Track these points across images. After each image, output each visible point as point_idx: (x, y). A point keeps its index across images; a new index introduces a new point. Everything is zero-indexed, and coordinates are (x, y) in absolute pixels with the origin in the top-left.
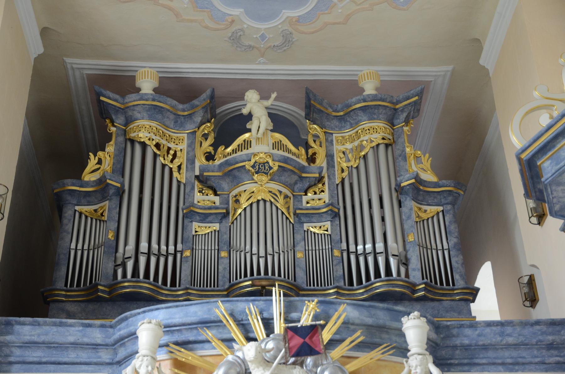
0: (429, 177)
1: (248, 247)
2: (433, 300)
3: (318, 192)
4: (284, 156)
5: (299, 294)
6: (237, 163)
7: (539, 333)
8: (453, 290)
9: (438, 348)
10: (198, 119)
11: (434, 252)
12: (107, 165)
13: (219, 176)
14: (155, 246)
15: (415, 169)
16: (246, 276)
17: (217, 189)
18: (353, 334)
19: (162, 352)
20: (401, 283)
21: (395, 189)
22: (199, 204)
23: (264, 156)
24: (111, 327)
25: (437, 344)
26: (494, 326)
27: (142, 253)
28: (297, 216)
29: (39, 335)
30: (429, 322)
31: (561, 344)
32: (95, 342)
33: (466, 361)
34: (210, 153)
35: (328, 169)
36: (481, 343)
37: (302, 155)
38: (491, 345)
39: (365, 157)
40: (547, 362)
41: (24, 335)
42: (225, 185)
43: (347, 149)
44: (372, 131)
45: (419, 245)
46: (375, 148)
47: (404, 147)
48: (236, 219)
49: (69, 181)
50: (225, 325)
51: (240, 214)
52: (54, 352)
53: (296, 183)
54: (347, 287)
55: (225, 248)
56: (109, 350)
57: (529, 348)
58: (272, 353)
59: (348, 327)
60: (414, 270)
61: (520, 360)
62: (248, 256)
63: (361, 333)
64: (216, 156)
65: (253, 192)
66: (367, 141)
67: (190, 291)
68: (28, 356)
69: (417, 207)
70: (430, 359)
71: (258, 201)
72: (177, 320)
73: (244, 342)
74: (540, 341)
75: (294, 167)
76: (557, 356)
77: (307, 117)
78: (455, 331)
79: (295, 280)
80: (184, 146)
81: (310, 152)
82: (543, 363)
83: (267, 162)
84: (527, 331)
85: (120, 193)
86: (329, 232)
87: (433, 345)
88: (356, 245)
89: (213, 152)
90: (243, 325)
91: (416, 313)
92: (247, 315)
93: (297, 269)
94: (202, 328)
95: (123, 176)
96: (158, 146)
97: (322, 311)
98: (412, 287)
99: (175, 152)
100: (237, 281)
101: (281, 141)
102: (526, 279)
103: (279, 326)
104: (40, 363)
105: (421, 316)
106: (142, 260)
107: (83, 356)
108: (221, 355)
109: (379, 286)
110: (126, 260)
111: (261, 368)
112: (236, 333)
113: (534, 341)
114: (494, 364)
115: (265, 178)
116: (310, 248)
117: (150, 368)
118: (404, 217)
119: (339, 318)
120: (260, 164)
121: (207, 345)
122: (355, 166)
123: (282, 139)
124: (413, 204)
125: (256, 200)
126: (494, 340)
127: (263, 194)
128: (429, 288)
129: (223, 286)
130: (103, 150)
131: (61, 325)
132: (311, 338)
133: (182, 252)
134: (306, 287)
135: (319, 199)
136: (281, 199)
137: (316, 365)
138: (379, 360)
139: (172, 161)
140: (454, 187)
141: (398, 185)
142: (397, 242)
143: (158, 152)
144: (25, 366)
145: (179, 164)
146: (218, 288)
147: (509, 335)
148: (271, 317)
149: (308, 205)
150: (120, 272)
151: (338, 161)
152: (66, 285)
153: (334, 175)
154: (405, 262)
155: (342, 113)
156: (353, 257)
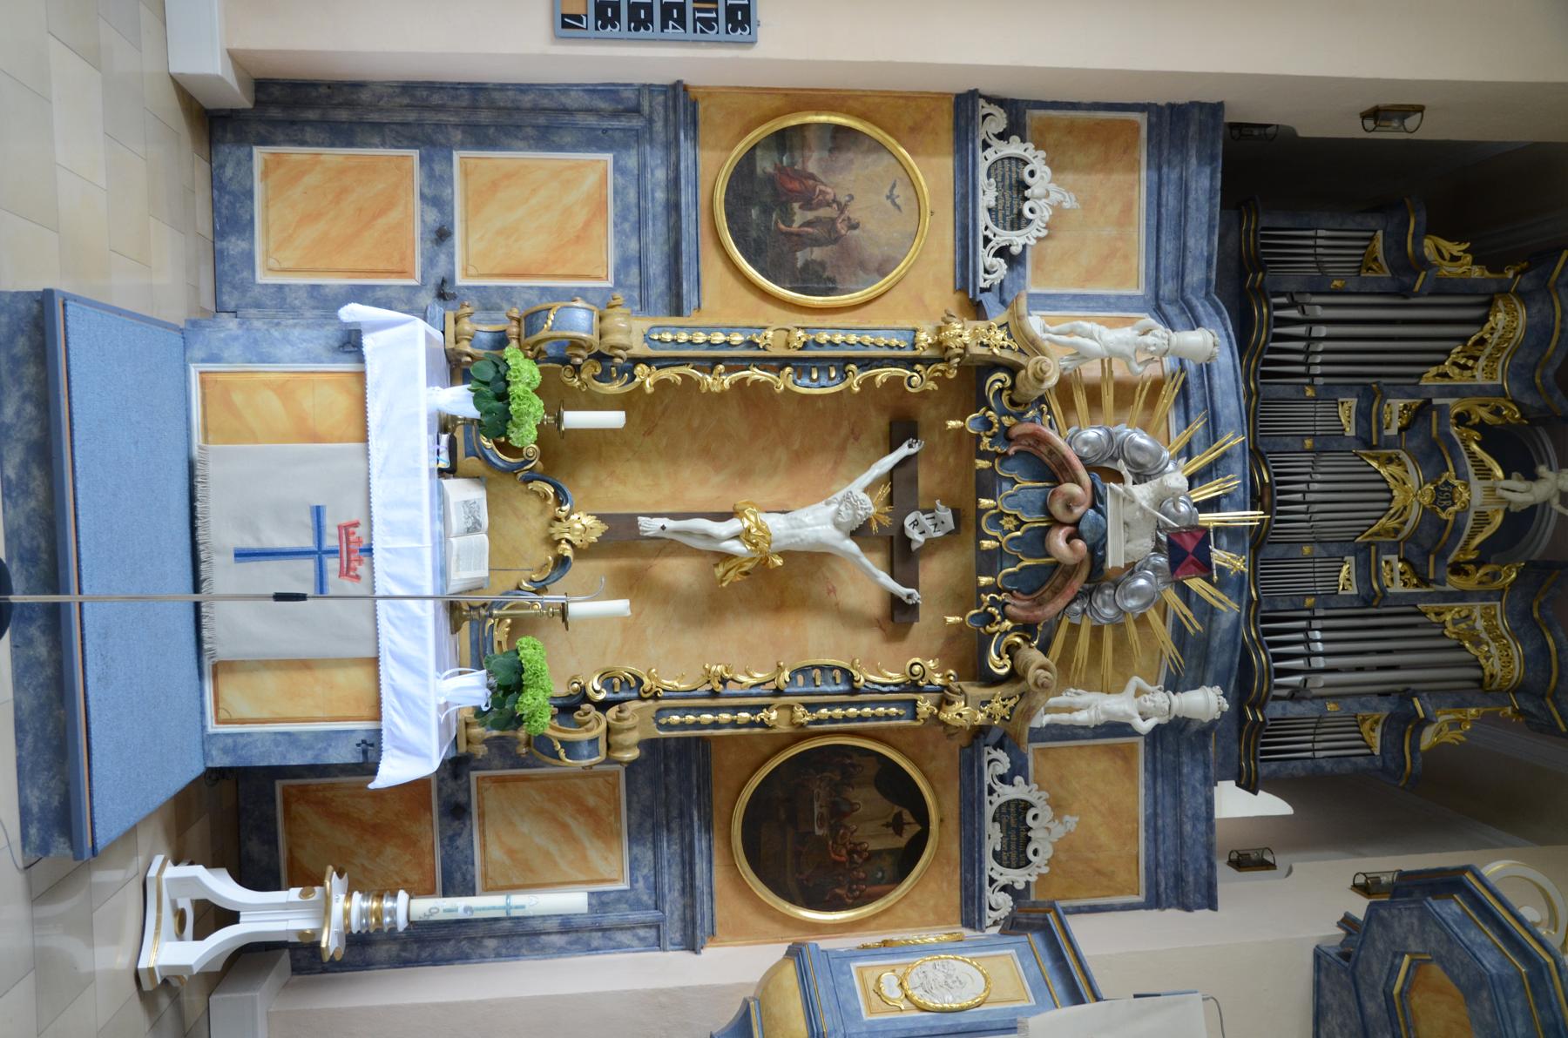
0: (1428, 738)
1: (1319, 477)
2: (1240, 731)
3: (1403, 578)
4: (1464, 529)
6: (1453, 460)
7: (1198, 866)
8: (1255, 759)
10: (1527, 400)
11: (1311, 737)
12: (1448, 270)
13: (1431, 434)
14: (1321, 346)
15: (1442, 719)
16: (1277, 474)
17: (1409, 431)
20: (1265, 689)
21: (1408, 689)
22: (1386, 406)
23: (1463, 499)
24: (1207, 294)
25: (1182, 731)
26: (1207, 809)
27: (1311, 329)
28: (1365, 547)
29: (1196, 200)
30: (1214, 722)
31: (1182, 892)
33: (1159, 767)
34: (1469, 418)
35: (1442, 592)
36: (1184, 789)
37: (1464, 554)
38: (1181, 801)
39: (1461, 648)
40: (1159, 870)
41: (1197, 181)
42: (1414, 443)
43: (1475, 621)
44: (1505, 659)
45: (1320, 717)
46: (1477, 663)
47: (1476, 706)
48: (1362, 460)
49: (1423, 217)
50: (1210, 446)
51: (1370, 465)
52: (1173, 223)
53: (1419, 545)
54: (1260, 615)
55: (1318, 445)
56: (1175, 294)
57: (1176, 850)
58: (1173, 510)
60: (1284, 708)
61: (1161, 837)
62: (1307, 478)
64: (1463, 428)
65: (1405, 484)
66: (1489, 651)
67: (1254, 399)
68: (1168, 190)
69: (1378, 720)
70: (1164, 720)
71: (1390, 491)
72: (1218, 382)
73: (1186, 473)
74: (1186, 866)
75: (1445, 544)
76: (1166, 884)
77: (1531, 564)
78: (1199, 756)
79: (1269, 543)
80: (1481, 379)
81: (1471, 568)
82: (1157, 866)
83: (1454, 504)
84: (1200, 851)
85: (1405, 291)
86: (1341, 592)
88: (1322, 630)
89: (1470, 423)
90: (1211, 471)
91: (1226, 706)
92: (1224, 476)
93: (1286, 546)
94: (1206, 415)
95: (1431, 294)
96: (1482, 342)
97: (1230, 580)
98: (1259, 704)
99: (1471, 368)
101: (1489, 524)
102: (1269, 858)
103: (1209, 519)
104: (1159, 206)
106: (1301, 330)
107: (1168, 261)
108: (1169, 443)
109: (1261, 659)
110: (1300, 307)
111: (1152, 495)
112: (1199, 462)
113: (1187, 859)
114: (1156, 803)
115: (1427, 500)
116: (1317, 565)
117: (1153, 348)
118: (1363, 699)
119: (1220, 601)
120: (1451, 493)
121: (1182, 423)
122: (1446, 633)
123: (1492, 525)
124: (1385, 714)
125: (1392, 487)
126: (1188, 806)
127: (1402, 497)
128: (1257, 727)
129: (1262, 444)
130: (1474, 262)
131: (1211, 228)
132: (1193, 562)
133: (1311, 385)
134: (1259, 558)
135: (1392, 579)
136: (1393, 524)
137: (1155, 568)
138: (1161, 652)
139: (1455, 364)
140: (1411, 773)
141: (1415, 693)
142: (1325, 686)
143: (1470, 343)
144: (1155, 187)
145: (1451, 374)
146: (1258, 438)
147: (1194, 826)
149: (1383, 563)
150: (1283, 300)
151: (1454, 607)
152: (1264, 229)
153: (1432, 601)
154: (1296, 695)
155: (1536, 615)
156: (1303, 624)
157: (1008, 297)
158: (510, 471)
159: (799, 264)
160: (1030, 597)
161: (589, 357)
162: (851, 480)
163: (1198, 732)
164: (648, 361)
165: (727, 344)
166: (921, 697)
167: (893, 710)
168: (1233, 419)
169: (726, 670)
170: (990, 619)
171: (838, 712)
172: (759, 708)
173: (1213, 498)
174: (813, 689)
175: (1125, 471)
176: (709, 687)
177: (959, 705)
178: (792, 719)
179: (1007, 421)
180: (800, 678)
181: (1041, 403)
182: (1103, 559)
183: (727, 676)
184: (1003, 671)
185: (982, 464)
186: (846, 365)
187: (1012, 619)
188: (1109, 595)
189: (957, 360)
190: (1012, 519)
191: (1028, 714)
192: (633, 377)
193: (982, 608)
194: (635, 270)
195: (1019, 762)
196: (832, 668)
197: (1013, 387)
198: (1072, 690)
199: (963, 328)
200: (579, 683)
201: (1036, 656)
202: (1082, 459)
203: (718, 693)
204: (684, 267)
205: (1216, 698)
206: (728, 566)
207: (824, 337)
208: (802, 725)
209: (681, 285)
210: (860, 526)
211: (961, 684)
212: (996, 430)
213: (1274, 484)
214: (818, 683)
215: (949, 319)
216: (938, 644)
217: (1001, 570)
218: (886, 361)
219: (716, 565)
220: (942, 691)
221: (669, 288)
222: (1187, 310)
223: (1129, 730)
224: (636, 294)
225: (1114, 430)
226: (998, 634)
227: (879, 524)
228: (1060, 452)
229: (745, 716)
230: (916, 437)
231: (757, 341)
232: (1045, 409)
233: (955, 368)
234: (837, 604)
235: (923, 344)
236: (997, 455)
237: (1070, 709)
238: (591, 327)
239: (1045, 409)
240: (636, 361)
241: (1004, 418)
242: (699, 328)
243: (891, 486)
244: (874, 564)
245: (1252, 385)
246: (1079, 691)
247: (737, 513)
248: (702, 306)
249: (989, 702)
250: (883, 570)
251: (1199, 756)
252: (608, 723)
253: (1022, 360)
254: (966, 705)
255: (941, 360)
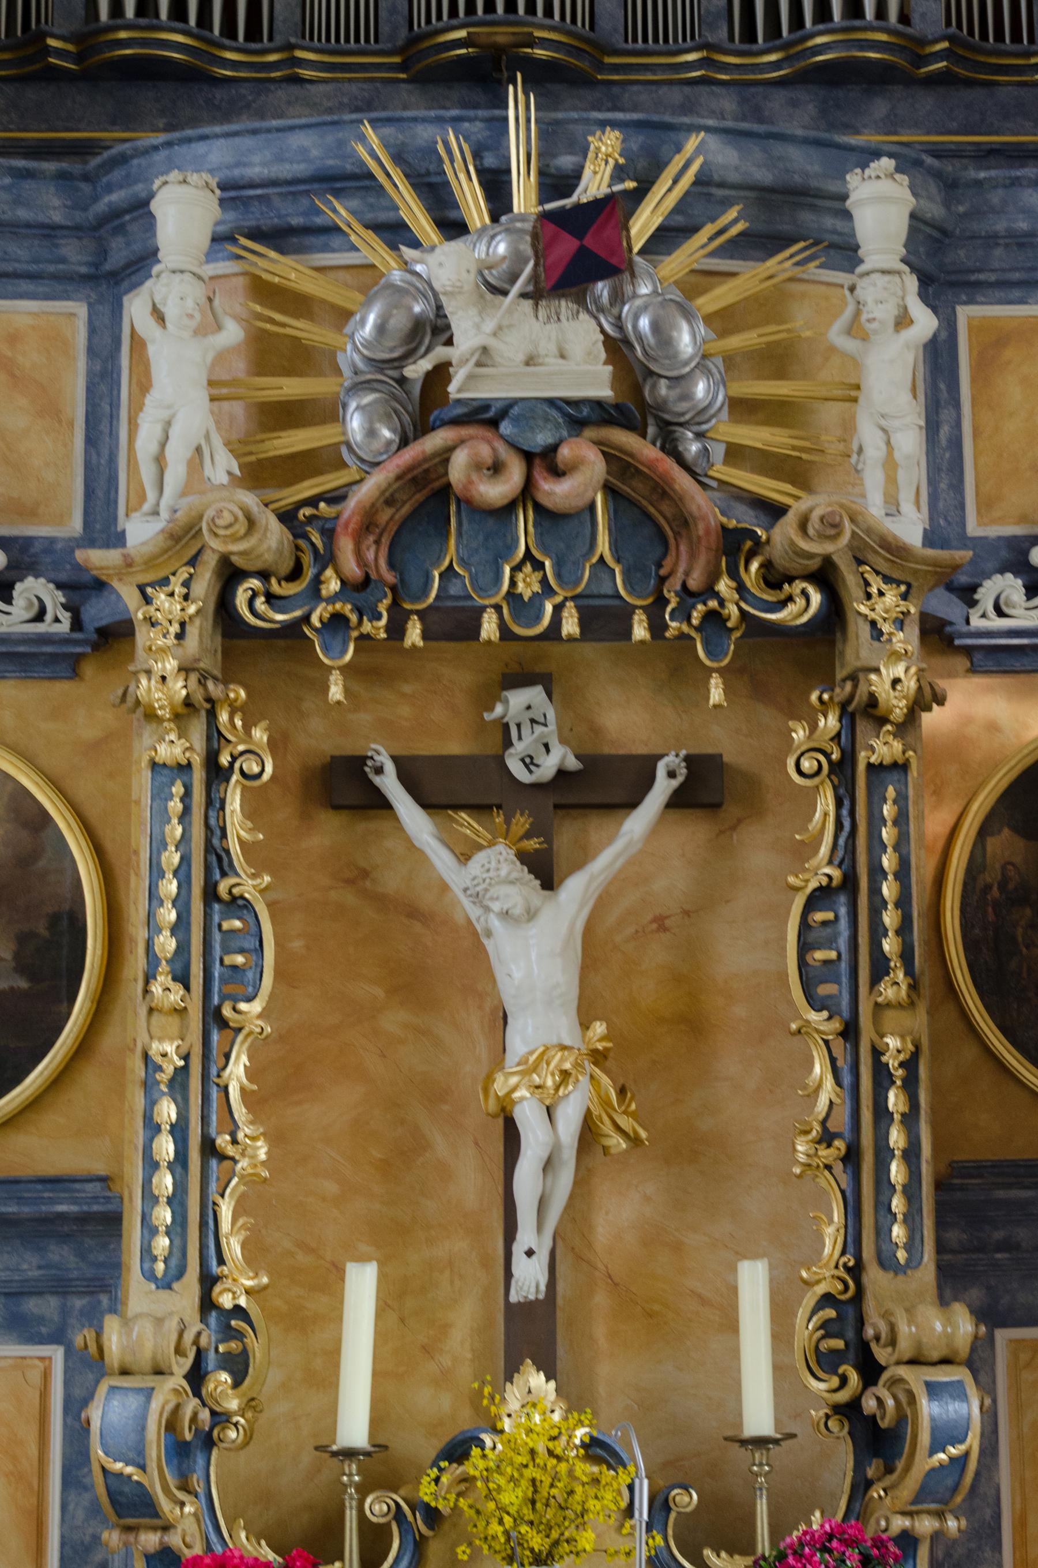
5: (602, 63)
9: (947, 241)
18: (724, 212)
19: (220, 255)
25: (944, 232)
32: (47, 221)
33: (1016, 276)
59: (710, 195)
63: (739, 213)
70: (912, 283)
72: (257, 170)
87: (935, 234)
94: (321, 195)
100: (430, 28)
105: (898, 169)
128: (960, 51)
148: (504, 167)
157: (85, 578)
158: (419, 1545)
159: (23, 984)
160: (672, 541)
161: (197, 1393)
162: (444, 887)
163: (947, 204)
164: (208, 1281)
165: (179, 1131)
166: (863, 757)
167: (888, 810)
168: (330, 139)
169: (807, 1132)
170: (714, 618)
171: (890, 918)
172: (882, 1077)
173: (481, 183)
174: (844, 966)
175: (425, 365)
176: (838, 1168)
177: (880, 685)
178: (900, 1006)
179: (332, 585)
180: (824, 990)
181: (296, 517)
182: (598, 404)
183: (817, 1128)
184: (816, 598)
185: (414, 634)
186: (218, 899)
187: (713, 577)
188: (669, 388)
189: (210, 685)
190: (520, 576)
191: (896, 550)
192: (238, 1311)
193: (693, 634)
194: (32, 1305)
195: (1004, 554)
196: (805, 925)
197: (264, 575)
198: (854, 458)
199: (149, 672)
200: (828, 1417)
201: (785, 531)
202: (404, 442)
203: (849, 1148)
204: (26, 1209)
205: (867, 183)
206: (607, 1128)
207: (167, 944)
208: (913, 987)
209: (62, 1216)
210: (530, 872)
211: (840, 675)
212: (349, 607)
213: (474, 18)
214: (833, 955)
215: (130, 700)
216: (767, 715)
217: (620, 597)
218: (213, 822)
219: (606, 1150)
220: (853, 716)
221: (64, 1238)
222: (116, 223)
223: (944, 335)
224: (78, 1303)
225: (348, 378)
226: (743, 605)
227: (528, 835)
228: (390, 485)
229: (894, 1100)
230: (363, 760)
231: (170, 1070)
232: (307, 511)
233: (227, 688)
234: (687, 913)
235: (177, 750)
236: (395, 604)
237: (890, 464)
238: (138, 1390)
239: (307, 511)
240: (207, 1304)
241: (324, 593)
242: (147, 1183)
243: (457, 807)
244: (611, 840)
245: (273, 58)
246: (855, 447)
247: (503, 1109)
248: (100, 1168)
249: (873, 623)
250: (621, 824)
251: (996, 197)
252: (898, 1363)
253: (210, 561)
254: (877, 670)
255: (212, 715)
